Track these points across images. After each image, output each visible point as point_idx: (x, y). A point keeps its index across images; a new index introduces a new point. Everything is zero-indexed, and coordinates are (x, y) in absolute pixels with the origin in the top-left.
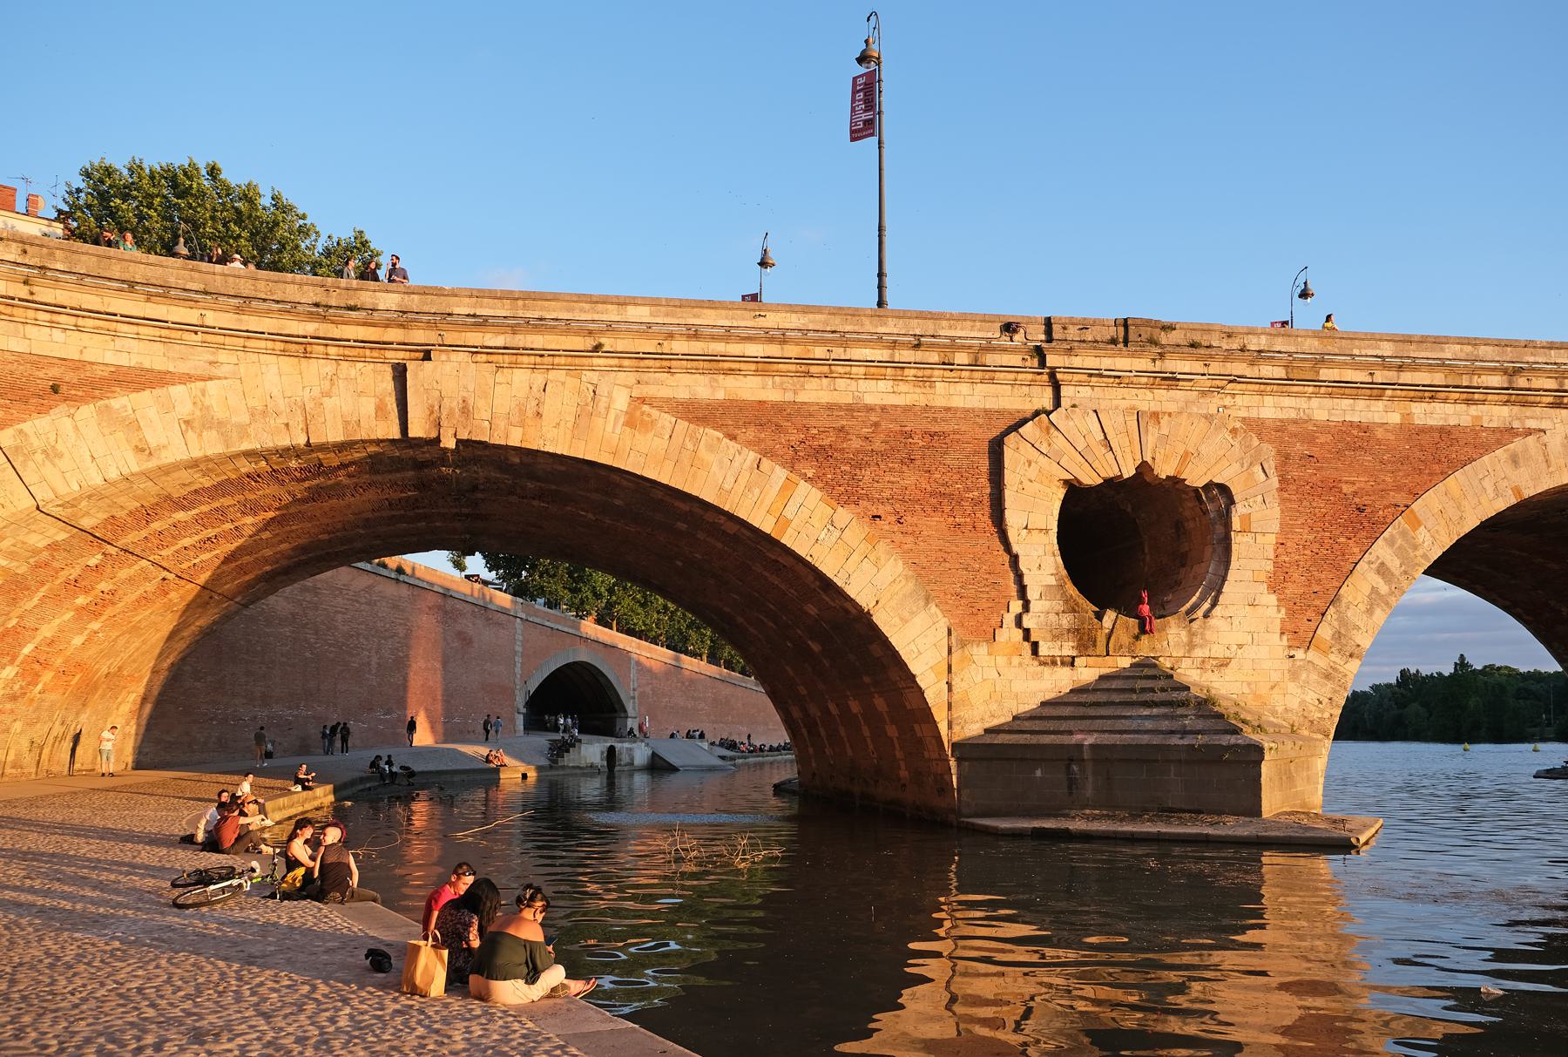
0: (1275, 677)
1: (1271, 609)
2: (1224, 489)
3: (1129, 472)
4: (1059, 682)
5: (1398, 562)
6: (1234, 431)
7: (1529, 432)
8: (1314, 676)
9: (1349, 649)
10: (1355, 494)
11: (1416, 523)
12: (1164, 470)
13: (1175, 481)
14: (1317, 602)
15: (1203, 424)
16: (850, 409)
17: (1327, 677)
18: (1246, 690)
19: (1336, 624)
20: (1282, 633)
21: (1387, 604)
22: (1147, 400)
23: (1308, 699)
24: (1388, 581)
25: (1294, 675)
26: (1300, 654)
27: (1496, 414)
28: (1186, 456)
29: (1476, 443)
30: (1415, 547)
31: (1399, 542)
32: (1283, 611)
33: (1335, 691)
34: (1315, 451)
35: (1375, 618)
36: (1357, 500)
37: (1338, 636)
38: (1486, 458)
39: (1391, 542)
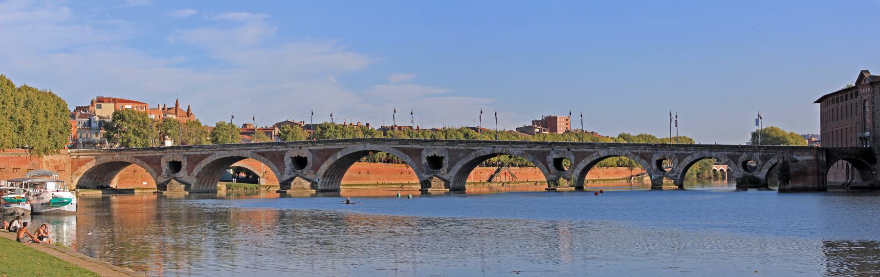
1: (186, 173)
3: (172, 160)
4: (166, 180)
12: (175, 160)
13: (176, 161)
16: (148, 156)
17: (191, 179)
22: (174, 153)
27: (211, 152)
29: (209, 155)
37: (193, 175)
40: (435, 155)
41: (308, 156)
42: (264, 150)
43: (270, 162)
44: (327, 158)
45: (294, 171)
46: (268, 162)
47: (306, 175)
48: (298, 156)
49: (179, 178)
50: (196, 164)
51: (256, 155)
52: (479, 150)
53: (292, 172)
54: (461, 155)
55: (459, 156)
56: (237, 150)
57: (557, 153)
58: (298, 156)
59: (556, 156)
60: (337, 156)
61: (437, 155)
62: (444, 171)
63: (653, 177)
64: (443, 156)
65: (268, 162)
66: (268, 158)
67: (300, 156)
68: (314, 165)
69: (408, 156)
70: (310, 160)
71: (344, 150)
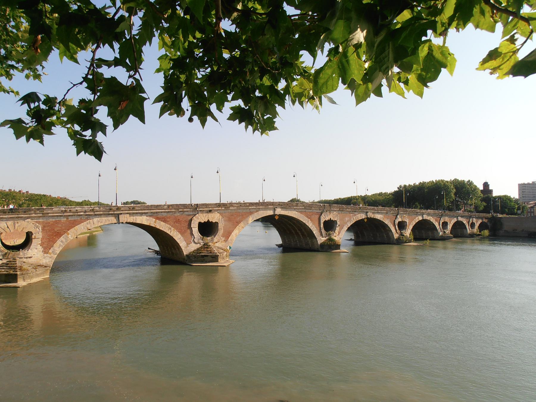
0: (41, 258)
1: (40, 248)
2: (31, 232)
5: (65, 240)
6: (33, 224)
7: (91, 219)
8: (48, 258)
9: (55, 254)
10: (57, 231)
11: (68, 234)
14: (49, 247)
15: (28, 223)
17: (51, 258)
18: (35, 261)
19: (53, 250)
20: (42, 252)
21: (63, 247)
23: (47, 261)
24: (63, 243)
25: (44, 258)
26: (46, 255)
28: (23, 228)
30: (68, 238)
31: (65, 237)
32: (43, 249)
33: (52, 260)
34: (50, 225)
35: (60, 249)
36: (58, 231)
37: (53, 252)
38: (82, 224)
39: (63, 237)
40: (330, 219)
41: (219, 221)
42: (165, 215)
43: (173, 229)
44: (238, 223)
45: (202, 240)
46: (170, 229)
47: (216, 242)
48: (208, 220)
49: (27, 258)
50: (59, 235)
51: (154, 220)
52: (358, 215)
53: (201, 241)
54: (347, 219)
55: (345, 220)
56: (127, 213)
57: (401, 217)
58: (208, 220)
59: (400, 220)
60: (248, 221)
61: (332, 219)
62: (336, 234)
63: (440, 234)
64: (336, 220)
65: (170, 229)
66: (170, 225)
67: (210, 221)
68: (224, 232)
69: (309, 220)
70: (221, 226)
71: (255, 214)
